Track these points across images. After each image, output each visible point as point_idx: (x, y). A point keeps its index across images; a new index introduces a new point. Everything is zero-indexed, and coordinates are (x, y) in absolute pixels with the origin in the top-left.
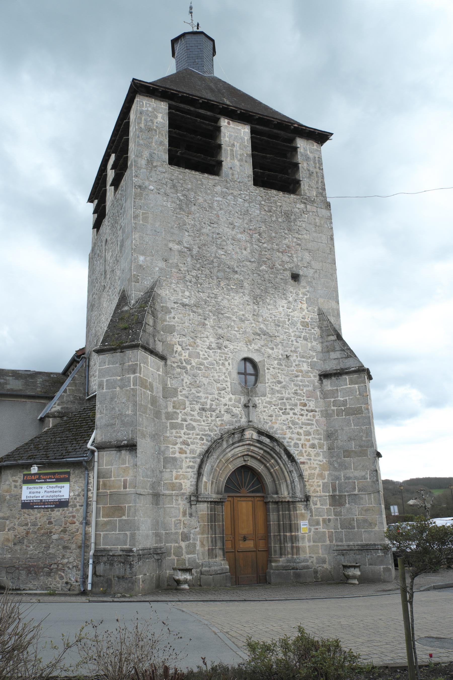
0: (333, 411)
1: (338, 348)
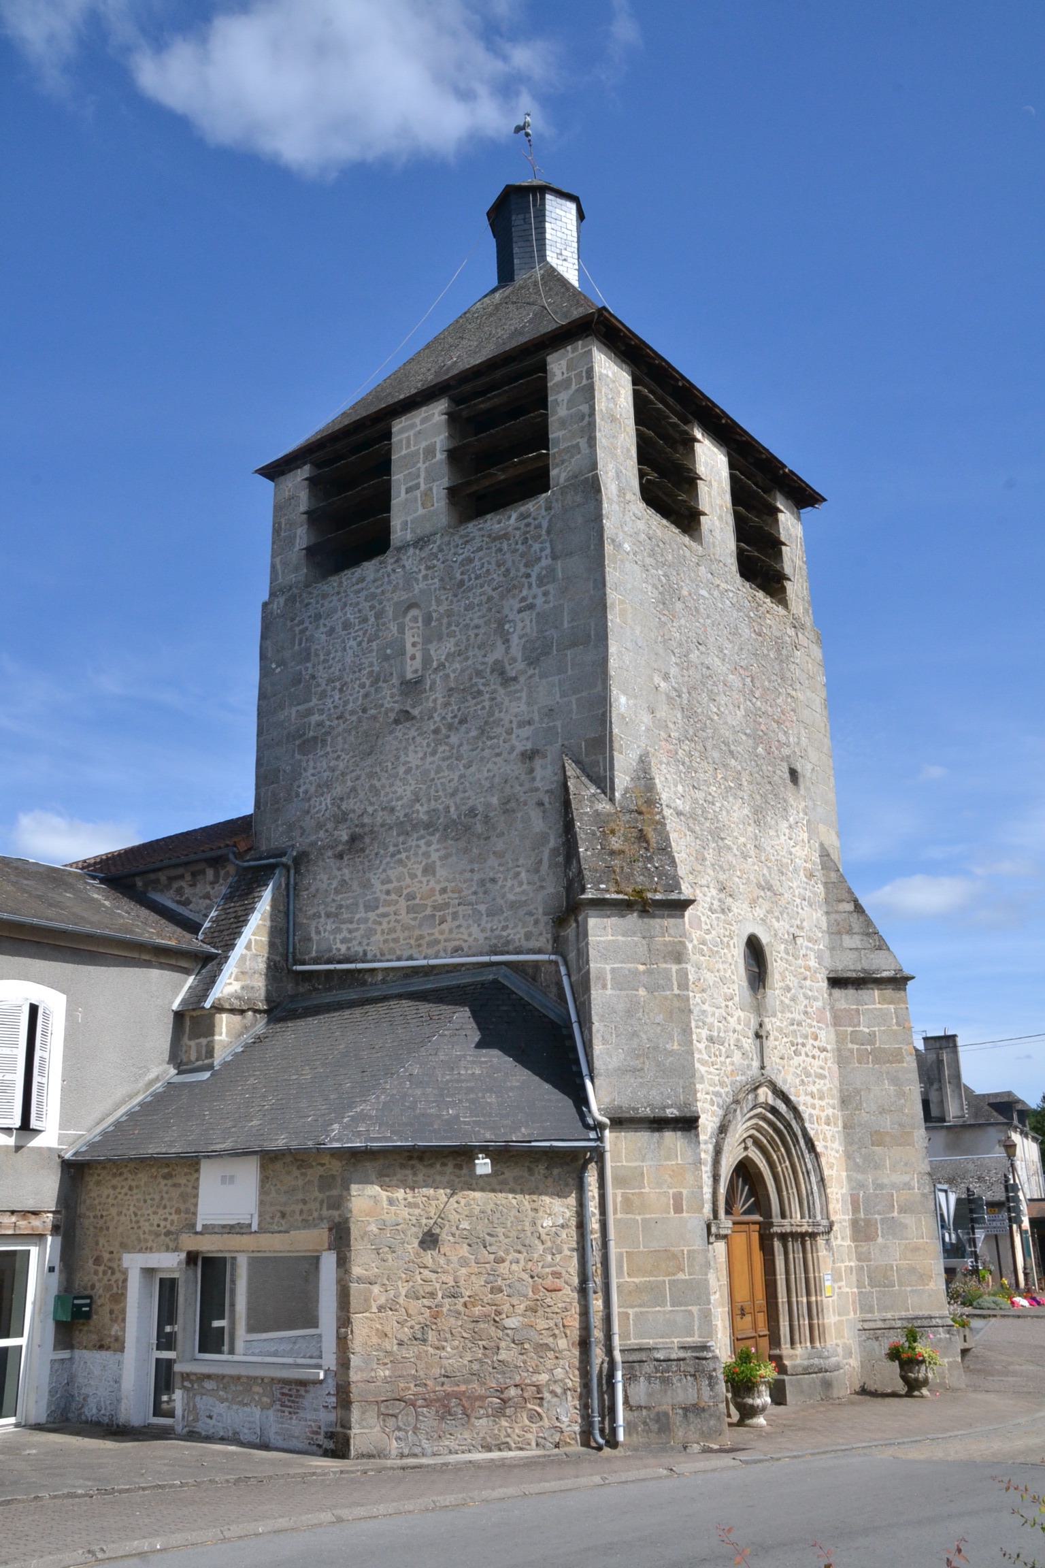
0: (851, 1051)
1: (856, 929)
